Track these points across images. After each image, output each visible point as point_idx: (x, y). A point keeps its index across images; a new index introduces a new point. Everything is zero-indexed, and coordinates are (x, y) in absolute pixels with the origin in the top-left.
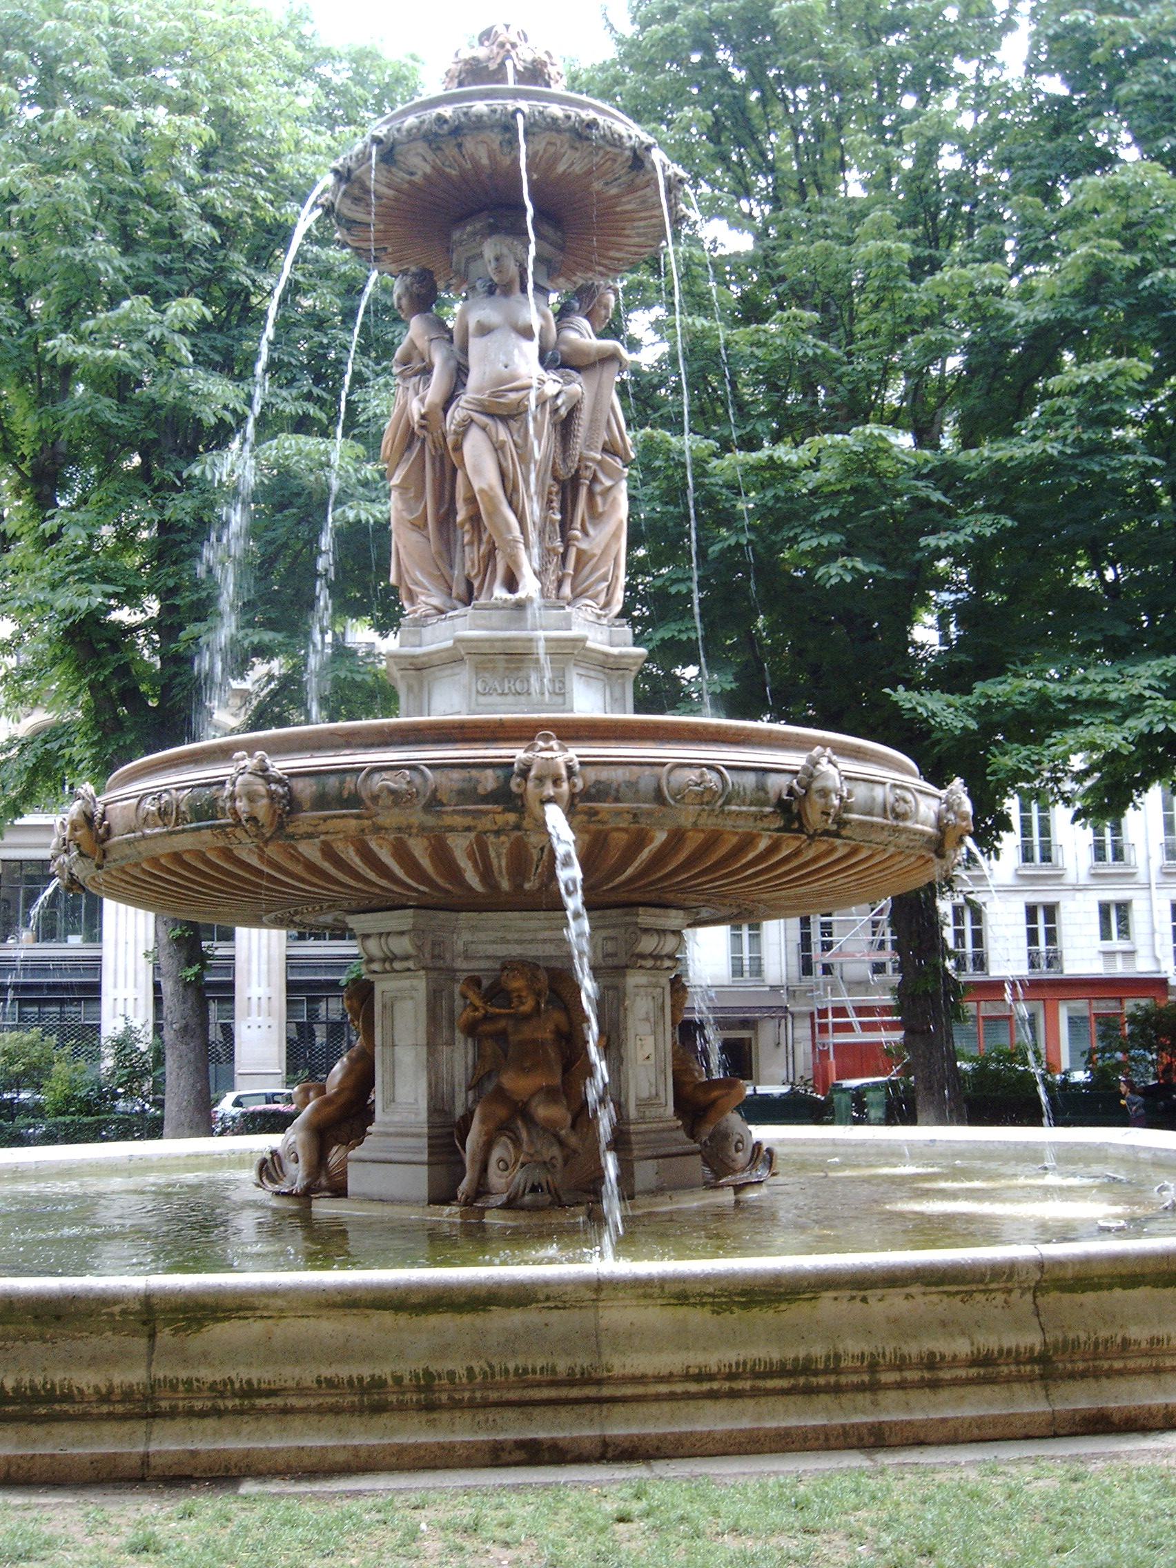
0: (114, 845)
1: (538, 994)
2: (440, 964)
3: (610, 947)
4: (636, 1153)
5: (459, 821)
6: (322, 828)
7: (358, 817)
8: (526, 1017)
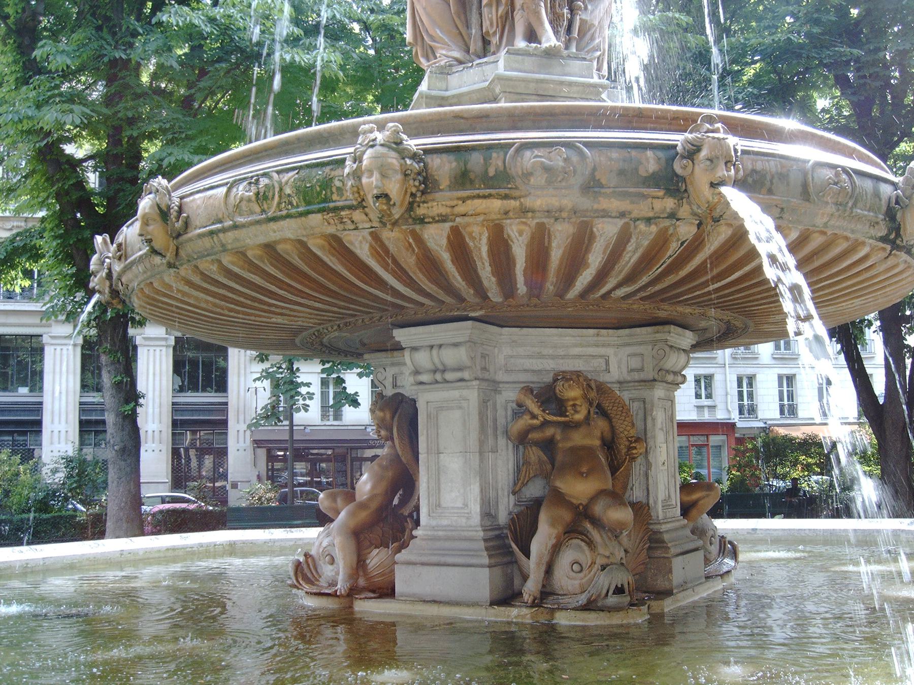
0: (191, 240)
1: (591, 404)
2: (486, 376)
3: (635, 363)
4: (673, 551)
5: (615, 205)
6: (458, 210)
7: (506, 197)
8: (576, 425)
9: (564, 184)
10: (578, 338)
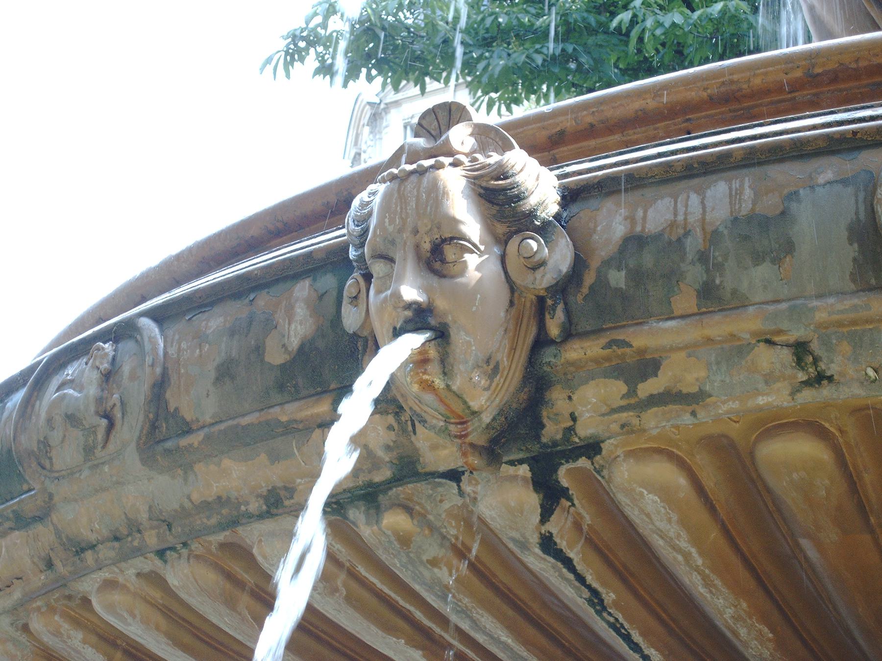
9: (111, 447)
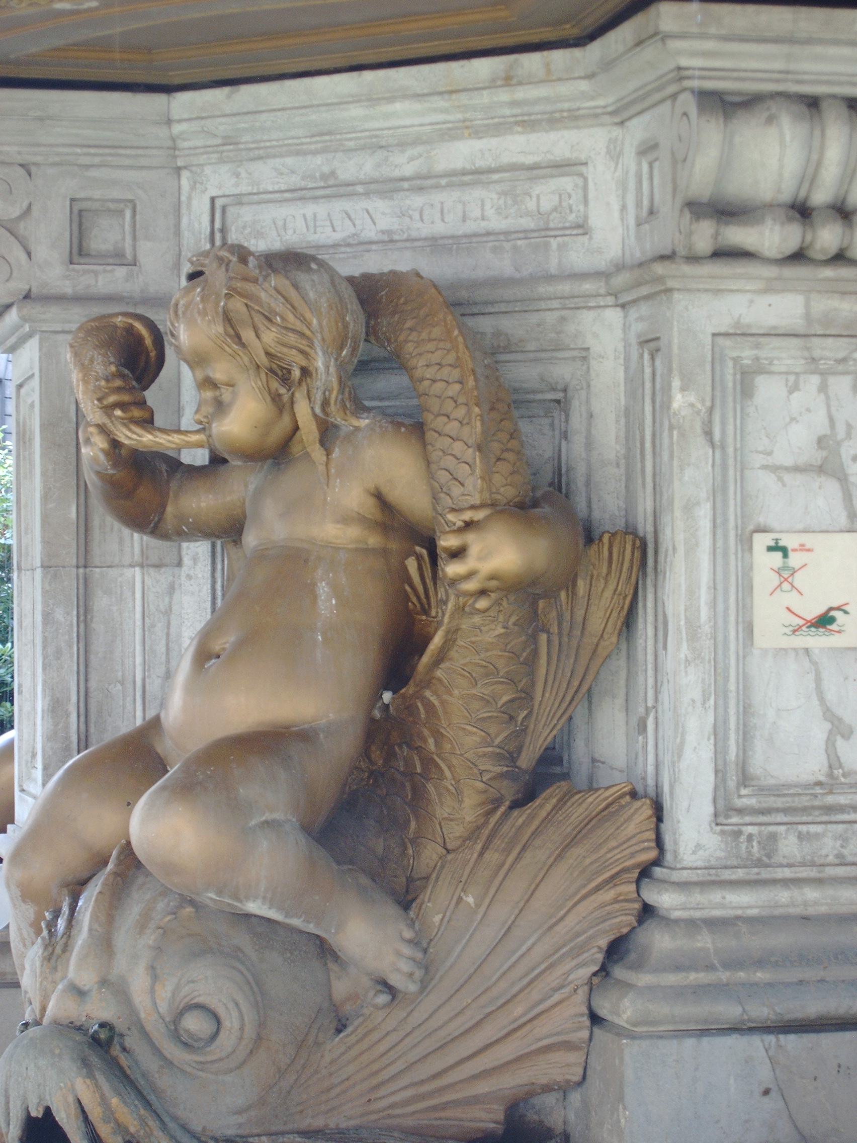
10: (439, 102)
